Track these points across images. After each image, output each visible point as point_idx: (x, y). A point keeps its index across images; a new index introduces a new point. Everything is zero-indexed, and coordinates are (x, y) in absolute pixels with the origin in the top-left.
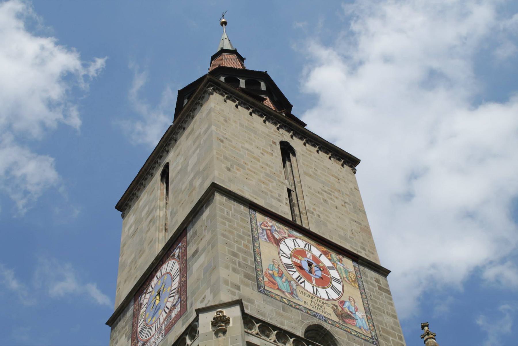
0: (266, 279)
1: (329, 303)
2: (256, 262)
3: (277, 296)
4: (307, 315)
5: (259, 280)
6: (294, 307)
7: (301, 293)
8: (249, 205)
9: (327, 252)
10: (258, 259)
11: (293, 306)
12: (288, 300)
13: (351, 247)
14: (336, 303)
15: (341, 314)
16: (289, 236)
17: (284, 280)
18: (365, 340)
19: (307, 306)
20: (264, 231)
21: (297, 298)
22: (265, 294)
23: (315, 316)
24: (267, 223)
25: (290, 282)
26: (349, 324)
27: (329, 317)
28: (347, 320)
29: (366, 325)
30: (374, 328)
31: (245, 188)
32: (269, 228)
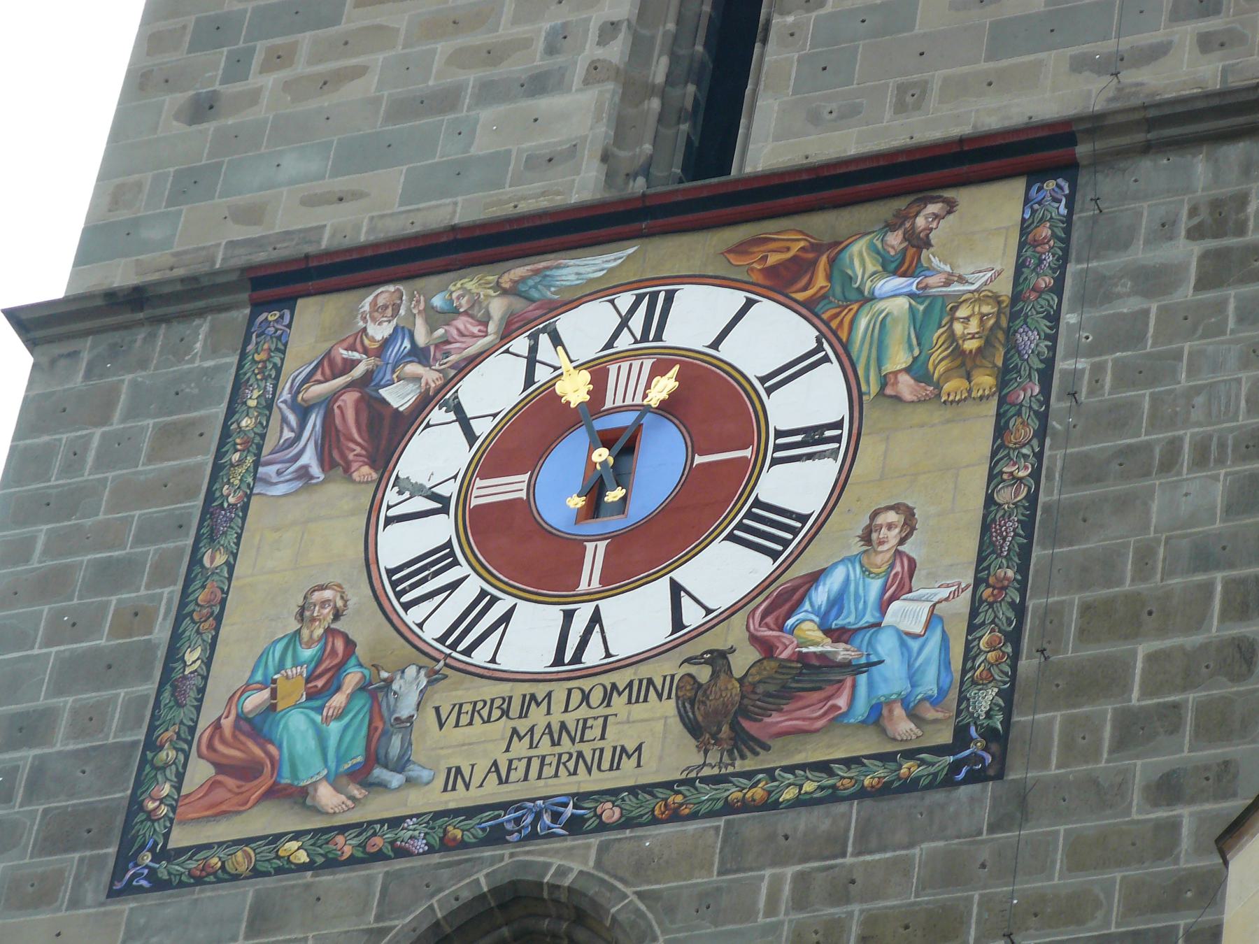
0: (199, 772)
1: (657, 671)
2: (167, 695)
3: (239, 854)
4: (436, 858)
5: (141, 808)
6: (352, 861)
7: (441, 725)
8: (245, 296)
9: (811, 256)
10: (192, 656)
11: (348, 851)
12: (317, 832)
13: (1080, 65)
14: (734, 635)
15: (737, 698)
16: (507, 335)
17: (339, 700)
18: (884, 791)
19: (460, 798)
20: (315, 420)
21: (396, 780)
22: (159, 885)
23: (496, 837)
24: (358, 340)
25: (389, 682)
26: (776, 744)
27: (628, 775)
28: (776, 718)
29: (946, 663)
30: (1009, 649)
31: (292, 165)
32: (358, 371)
